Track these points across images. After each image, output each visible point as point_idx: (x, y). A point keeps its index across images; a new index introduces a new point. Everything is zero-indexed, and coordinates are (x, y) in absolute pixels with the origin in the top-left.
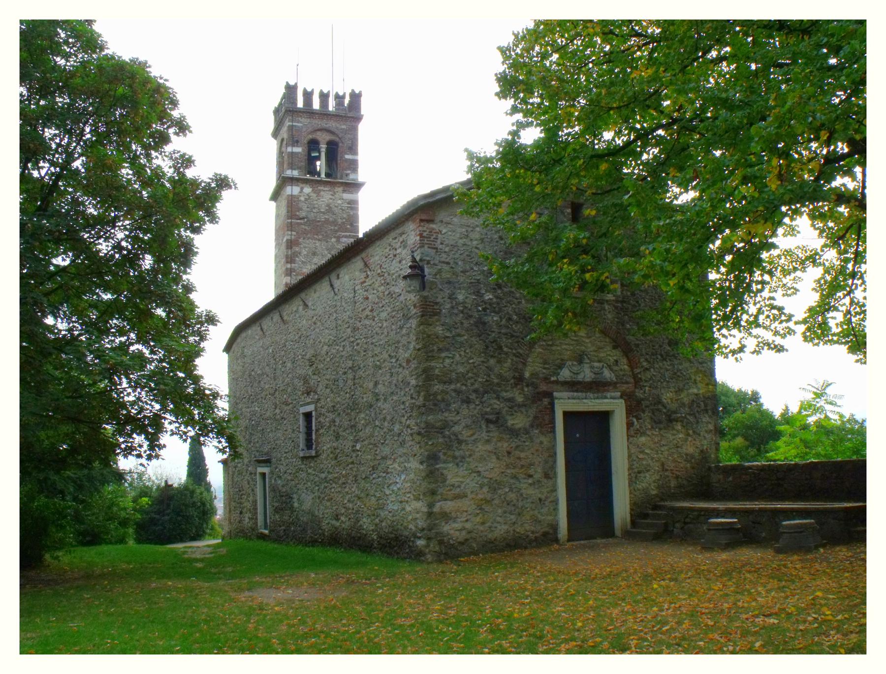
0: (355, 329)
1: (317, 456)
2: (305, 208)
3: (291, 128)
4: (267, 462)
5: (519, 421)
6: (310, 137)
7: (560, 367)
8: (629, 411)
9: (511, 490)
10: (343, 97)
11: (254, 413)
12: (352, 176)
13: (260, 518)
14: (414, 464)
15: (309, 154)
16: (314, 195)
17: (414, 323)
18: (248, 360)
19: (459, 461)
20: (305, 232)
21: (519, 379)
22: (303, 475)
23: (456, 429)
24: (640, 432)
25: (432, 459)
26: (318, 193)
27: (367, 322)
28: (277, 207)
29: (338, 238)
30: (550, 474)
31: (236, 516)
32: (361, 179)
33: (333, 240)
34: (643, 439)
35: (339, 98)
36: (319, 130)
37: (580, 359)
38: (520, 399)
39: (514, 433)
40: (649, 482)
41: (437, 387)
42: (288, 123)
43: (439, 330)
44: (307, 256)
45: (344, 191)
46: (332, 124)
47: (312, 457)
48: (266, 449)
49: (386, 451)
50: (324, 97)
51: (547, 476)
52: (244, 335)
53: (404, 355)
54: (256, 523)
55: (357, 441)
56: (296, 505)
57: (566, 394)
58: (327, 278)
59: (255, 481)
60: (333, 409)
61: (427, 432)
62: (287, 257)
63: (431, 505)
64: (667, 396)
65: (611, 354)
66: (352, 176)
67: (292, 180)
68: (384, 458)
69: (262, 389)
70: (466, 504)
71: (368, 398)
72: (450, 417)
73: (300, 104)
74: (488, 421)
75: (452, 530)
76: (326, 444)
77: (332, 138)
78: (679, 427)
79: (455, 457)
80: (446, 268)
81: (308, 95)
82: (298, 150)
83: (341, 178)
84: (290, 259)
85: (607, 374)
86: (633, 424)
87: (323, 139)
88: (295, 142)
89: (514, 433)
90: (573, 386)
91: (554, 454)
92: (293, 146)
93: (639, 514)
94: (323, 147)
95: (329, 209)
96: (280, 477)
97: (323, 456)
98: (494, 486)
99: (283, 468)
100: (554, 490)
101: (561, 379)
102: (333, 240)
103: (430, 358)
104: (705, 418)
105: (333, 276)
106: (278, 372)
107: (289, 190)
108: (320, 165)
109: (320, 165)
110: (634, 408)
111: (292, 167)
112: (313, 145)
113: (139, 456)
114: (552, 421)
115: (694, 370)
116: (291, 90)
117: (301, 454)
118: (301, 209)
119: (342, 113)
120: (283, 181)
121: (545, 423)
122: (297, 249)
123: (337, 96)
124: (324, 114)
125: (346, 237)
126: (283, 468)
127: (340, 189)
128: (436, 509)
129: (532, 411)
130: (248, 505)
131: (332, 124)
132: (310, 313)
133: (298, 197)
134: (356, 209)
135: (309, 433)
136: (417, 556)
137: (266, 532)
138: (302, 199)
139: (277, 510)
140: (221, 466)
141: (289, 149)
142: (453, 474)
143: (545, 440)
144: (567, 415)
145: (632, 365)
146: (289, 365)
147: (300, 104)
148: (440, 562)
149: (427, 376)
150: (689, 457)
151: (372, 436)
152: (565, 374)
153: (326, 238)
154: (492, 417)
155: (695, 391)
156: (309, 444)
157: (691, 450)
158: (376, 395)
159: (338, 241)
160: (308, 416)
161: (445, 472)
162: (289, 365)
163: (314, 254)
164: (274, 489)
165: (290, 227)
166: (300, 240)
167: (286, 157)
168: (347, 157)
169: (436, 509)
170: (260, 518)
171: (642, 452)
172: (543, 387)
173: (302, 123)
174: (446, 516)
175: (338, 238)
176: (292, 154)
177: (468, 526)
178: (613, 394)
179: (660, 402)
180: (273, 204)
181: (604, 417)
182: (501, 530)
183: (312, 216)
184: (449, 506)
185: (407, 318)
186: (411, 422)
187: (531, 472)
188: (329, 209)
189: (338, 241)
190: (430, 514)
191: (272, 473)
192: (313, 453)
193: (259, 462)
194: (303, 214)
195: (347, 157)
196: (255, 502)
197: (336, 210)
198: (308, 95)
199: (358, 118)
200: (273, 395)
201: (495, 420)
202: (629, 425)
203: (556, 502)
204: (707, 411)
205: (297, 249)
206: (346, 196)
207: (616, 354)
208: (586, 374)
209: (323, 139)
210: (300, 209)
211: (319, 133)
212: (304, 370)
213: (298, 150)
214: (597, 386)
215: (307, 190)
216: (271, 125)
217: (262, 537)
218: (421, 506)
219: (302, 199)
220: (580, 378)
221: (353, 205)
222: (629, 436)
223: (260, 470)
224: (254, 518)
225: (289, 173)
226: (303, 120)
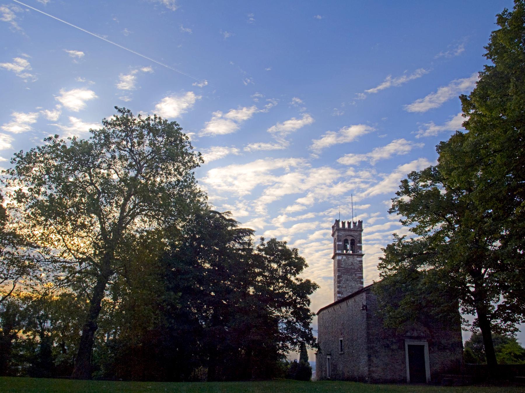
0: (353, 318)
1: (344, 354)
2: (344, 264)
3: (338, 236)
4: (330, 355)
5: (394, 347)
6: (345, 238)
7: (407, 332)
9: (392, 366)
10: (356, 223)
11: (326, 339)
13: (328, 373)
15: (345, 244)
17: (365, 319)
18: (325, 320)
19: (377, 357)
22: (340, 359)
23: (376, 348)
24: (433, 352)
25: (369, 356)
28: (334, 262)
29: (356, 274)
30: (404, 362)
33: (354, 275)
34: (435, 354)
36: (348, 236)
37: (413, 330)
38: (394, 341)
40: (437, 367)
41: (371, 337)
42: (336, 234)
43: (371, 322)
45: (357, 257)
46: (352, 233)
47: (342, 354)
48: (330, 350)
49: (360, 353)
51: (403, 363)
52: (323, 312)
53: (363, 328)
54: (326, 375)
56: (338, 369)
57: (408, 340)
58: (345, 301)
61: (368, 348)
62: (338, 281)
63: (369, 368)
64: (443, 341)
65: (423, 328)
66: (360, 252)
67: (339, 254)
68: (359, 355)
71: (355, 338)
72: (375, 345)
74: (385, 347)
75: (375, 376)
76: (346, 351)
77: (353, 238)
78: (448, 351)
79: (376, 356)
80: (373, 305)
81: (343, 223)
82: (341, 243)
83: (356, 253)
84: (339, 282)
85: (422, 334)
86: (431, 349)
88: (339, 241)
89: (393, 350)
90: (411, 338)
91: (405, 357)
92: (339, 242)
94: (349, 242)
95: (352, 264)
96: (334, 360)
97: (345, 354)
100: (405, 367)
101: (407, 335)
103: (369, 329)
104: (458, 349)
105: (347, 301)
106: (333, 327)
107: (338, 258)
108: (349, 246)
109: (349, 246)
110: (431, 344)
111: (339, 250)
112: (346, 241)
113: (296, 351)
115: (453, 333)
116: (337, 222)
117: (340, 353)
118: (342, 264)
119: (356, 229)
120: (336, 255)
122: (341, 279)
123: (354, 223)
124: (349, 229)
125: (358, 274)
126: (334, 357)
127: (356, 257)
128: (371, 369)
129: (398, 344)
130: (324, 369)
131: (352, 233)
132: (342, 310)
135: (342, 347)
137: (329, 378)
138: (343, 261)
139: (333, 371)
141: (338, 243)
143: (402, 353)
144: (409, 346)
145: (431, 332)
146: (336, 325)
147: (341, 226)
148: (371, 384)
150: (451, 361)
152: (408, 334)
153: (351, 274)
154: (386, 345)
155: (454, 340)
157: (453, 358)
159: (356, 276)
160: (341, 341)
161: (373, 360)
162: (336, 325)
163: (347, 280)
164: (331, 364)
165: (339, 271)
166: (342, 275)
167: (337, 246)
168: (358, 245)
169: (371, 369)
170: (328, 373)
171: (435, 358)
172: (401, 338)
173: (342, 233)
174: (373, 372)
175: (356, 274)
176: (339, 245)
177: (379, 375)
178: (424, 340)
179: (441, 343)
180: (333, 260)
181: (423, 346)
182: (389, 377)
183: (346, 267)
184: (374, 369)
185: (364, 318)
186: (365, 346)
187: (398, 361)
188: (352, 264)
189: (356, 276)
190: (369, 371)
192: (343, 352)
193: (328, 354)
194: (343, 266)
195: (358, 245)
196: (326, 368)
197: (355, 264)
198: (343, 223)
201: (387, 346)
202: (430, 350)
203: (406, 370)
204: (459, 347)
205: (341, 279)
206: (359, 259)
207: (426, 329)
208: (415, 334)
209: (349, 238)
211: (348, 237)
213: (341, 243)
214: (419, 338)
215: (344, 257)
217: (328, 379)
219: (343, 261)
221: (361, 262)
222: (430, 353)
225: (337, 252)
226: (342, 232)
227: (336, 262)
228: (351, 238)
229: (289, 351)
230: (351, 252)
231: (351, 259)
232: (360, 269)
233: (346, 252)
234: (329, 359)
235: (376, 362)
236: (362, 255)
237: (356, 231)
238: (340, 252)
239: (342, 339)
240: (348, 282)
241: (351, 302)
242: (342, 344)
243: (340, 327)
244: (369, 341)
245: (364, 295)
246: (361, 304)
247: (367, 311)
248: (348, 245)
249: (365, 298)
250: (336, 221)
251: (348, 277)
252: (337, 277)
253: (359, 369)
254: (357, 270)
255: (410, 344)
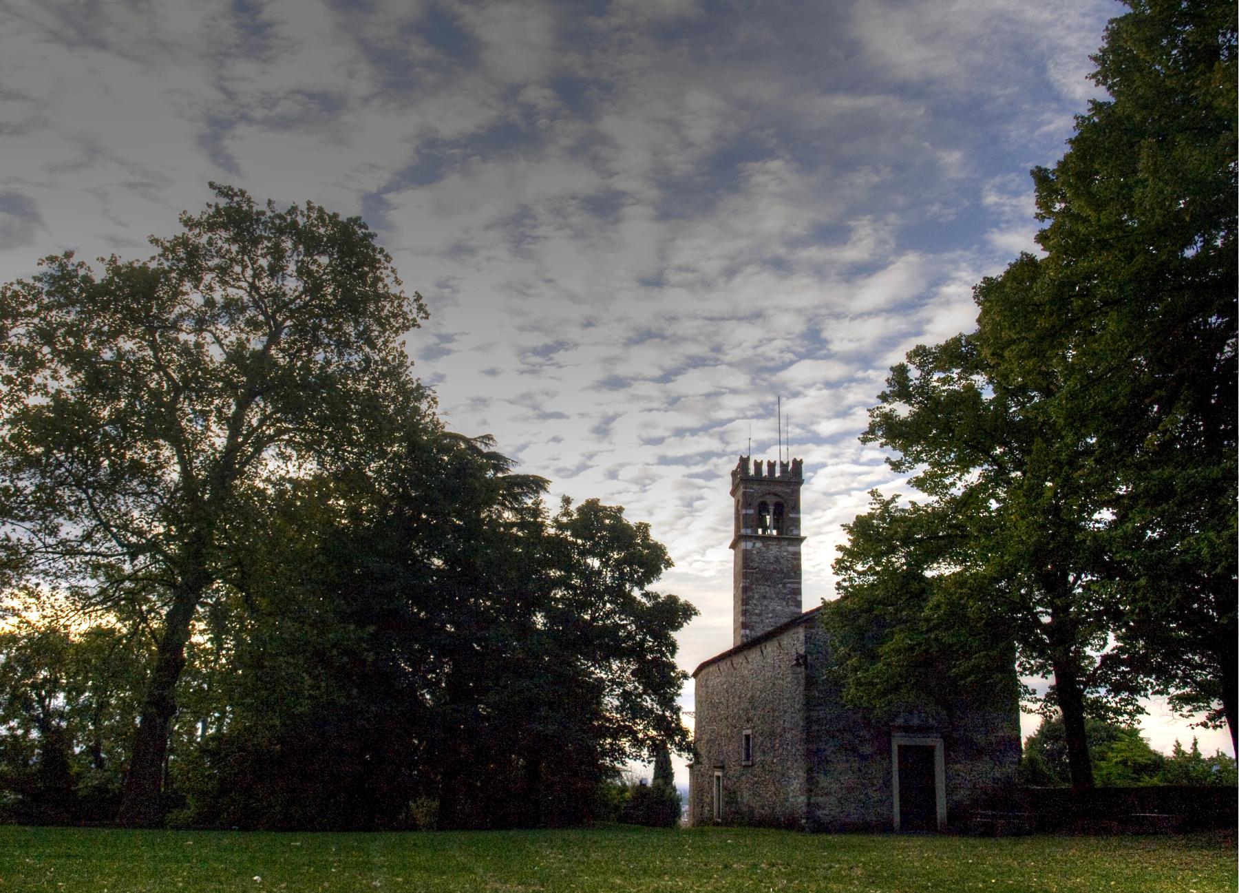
0: (774, 684)
1: (753, 765)
3: (744, 493)
4: (722, 768)
7: (896, 716)
8: (948, 748)
12: (795, 532)
14: (801, 773)
16: (764, 549)
17: (802, 688)
20: (757, 579)
21: (868, 724)
25: (810, 771)
26: (767, 547)
27: (781, 682)
28: (735, 555)
30: (887, 784)
31: (698, 810)
32: (802, 535)
33: (780, 586)
35: (784, 466)
39: (863, 758)
40: (962, 794)
41: (815, 727)
44: (758, 600)
45: (789, 545)
46: (778, 489)
50: (771, 466)
52: (706, 671)
55: (774, 757)
59: (712, 781)
60: (761, 734)
61: (809, 754)
62: (743, 600)
63: (809, 799)
64: (979, 738)
66: (795, 532)
69: (720, 714)
70: (832, 799)
71: (779, 730)
73: (752, 471)
76: (758, 758)
77: (779, 500)
81: (758, 466)
82: (751, 512)
84: (745, 602)
87: (771, 500)
89: (863, 758)
90: (907, 729)
93: (952, 815)
94: (771, 509)
95: (777, 560)
98: (851, 789)
99: (731, 773)
102: (780, 586)
107: (743, 545)
111: (746, 527)
113: (643, 761)
114: (889, 751)
116: (744, 462)
119: (786, 480)
121: (885, 751)
124: (771, 479)
125: (791, 583)
126: (731, 773)
127: (786, 543)
131: (778, 489)
133: (750, 551)
134: (799, 559)
135: (747, 749)
136: (801, 829)
139: (727, 803)
140: (688, 769)
142: (824, 781)
144: (900, 747)
146: (737, 700)
147: (752, 471)
149: (808, 720)
151: (782, 754)
152: (900, 721)
156: (748, 757)
157: (998, 775)
158: (784, 729)
160: (747, 737)
163: (765, 597)
164: (725, 788)
165: (745, 576)
169: (812, 801)
174: (818, 806)
180: (732, 551)
181: (930, 751)
182: (854, 817)
186: (800, 748)
190: (809, 804)
191: (724, 776)
194: (756, 565)
196: (712, 797)
197: (782, 560)
199: (800, 482)
200: (726, 719)
202: (947, 756)
206: (791, 549)
208: (916, 721)
209: (771, 500)
210: (752, 561)
212: (746, 705)
213: (751, 512)
214: (924, 730)
215: (759, 545)
216: (730, 488)
217: (717, 824)
218: (802, 799)
220: (911, 723)
221: (797, 556)
223: (716, 773)
224: (711, 810)
225: (743, 531)
227: (740, 555)
228: (774, 499)
229: (627, 760)
230: (775, 532)
231: (774, 550)
232: (795, 573)
233: (764, 532)
234: (718, 778)
235: (825, 785)
236: (801, 540)
237: (788, 484)
238: (749, 532)
239: (749, 732)
240: (765, 602)
241: (770, 648)
242: (748, 744)
243: (746, 705)
244: (810, 736)
245: (801, 633)
246: (793, 652)
247: (806, 668)
248: (768, 517)
249: (802, 638)
250: (742, 459)
251: (768, 589)
252: (740, 590)
253: (786, 800)
254: (787, 576)
255: (902, 743)
